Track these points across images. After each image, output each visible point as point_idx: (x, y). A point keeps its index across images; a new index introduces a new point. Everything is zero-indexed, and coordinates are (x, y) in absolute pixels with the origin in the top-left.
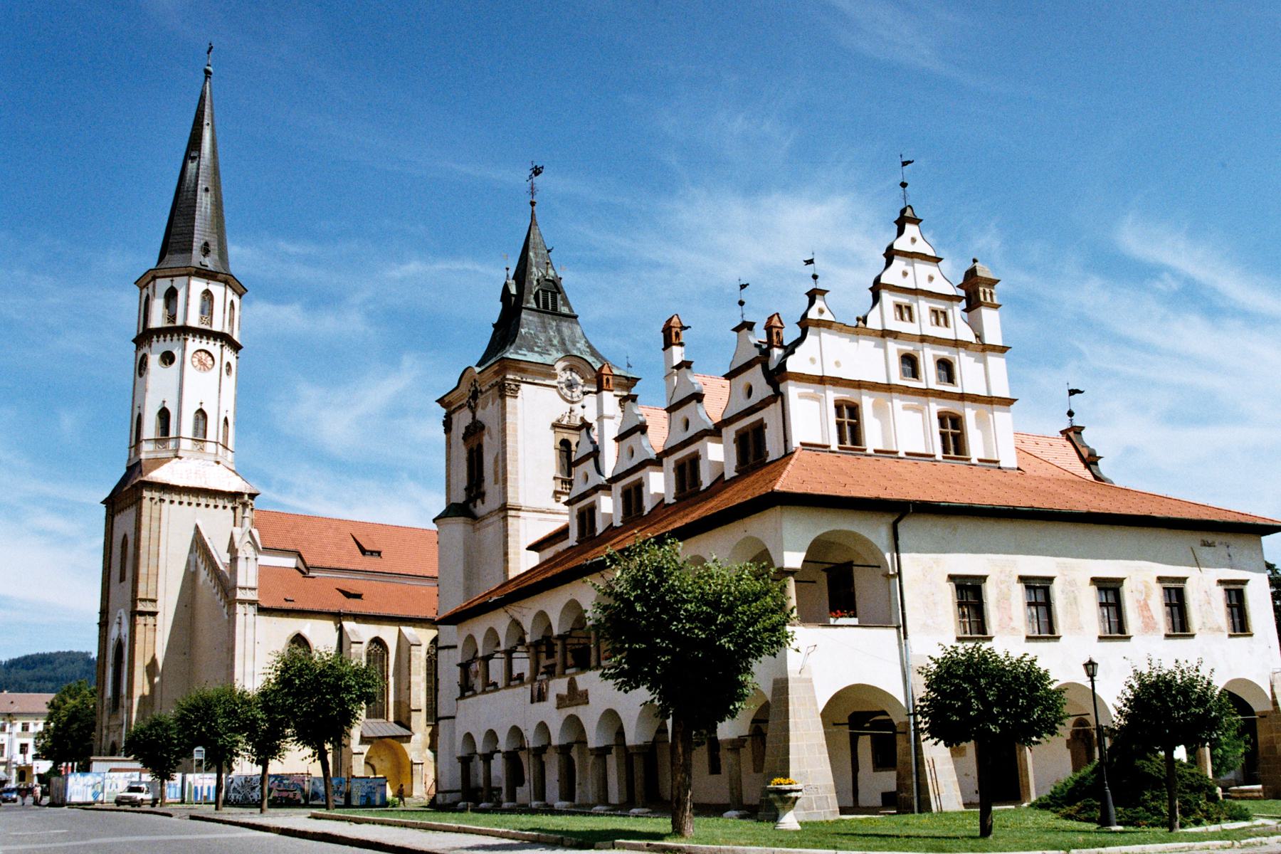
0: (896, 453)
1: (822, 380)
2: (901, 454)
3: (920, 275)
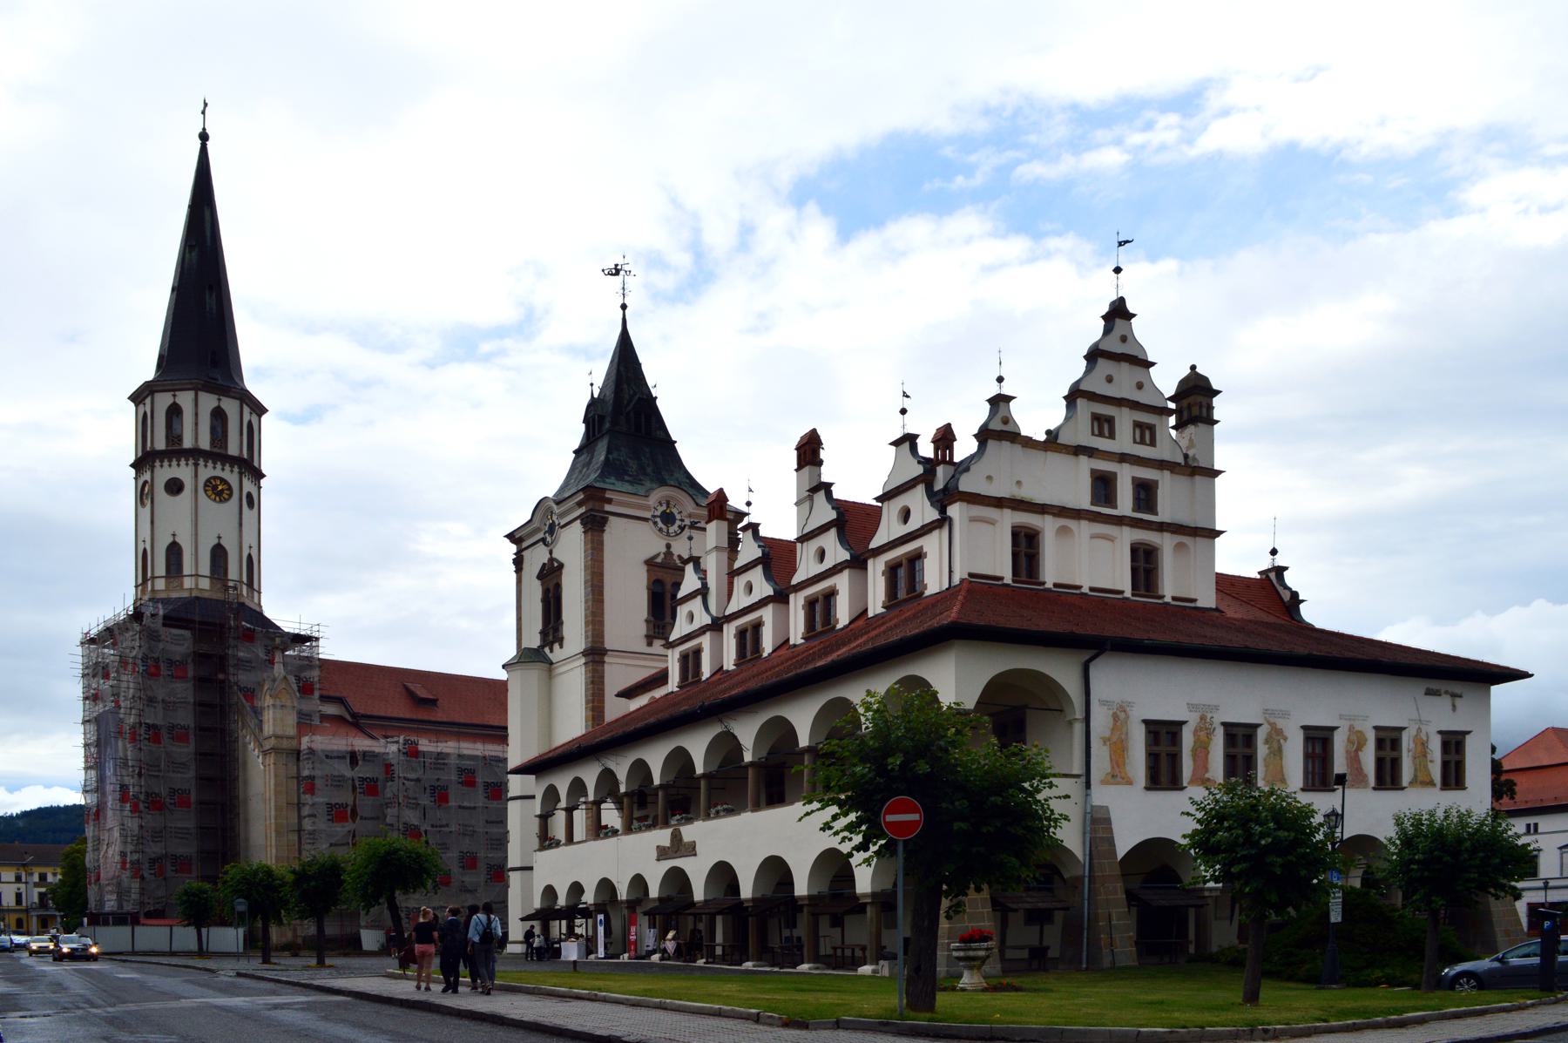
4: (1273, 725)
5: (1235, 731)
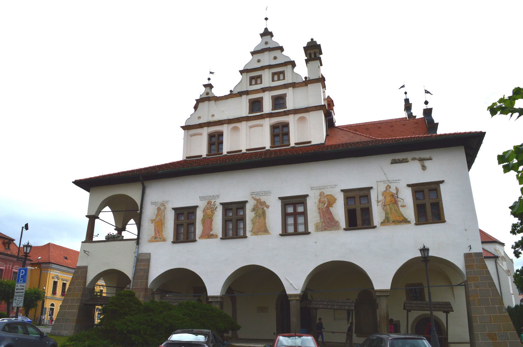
0: (241, 151)
1: (201, 126)
2: (244, 151)
3: (267, 59)
4: (258, 201)
5: (230, 207)
